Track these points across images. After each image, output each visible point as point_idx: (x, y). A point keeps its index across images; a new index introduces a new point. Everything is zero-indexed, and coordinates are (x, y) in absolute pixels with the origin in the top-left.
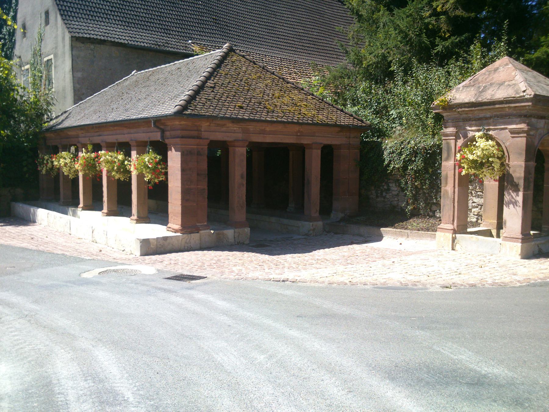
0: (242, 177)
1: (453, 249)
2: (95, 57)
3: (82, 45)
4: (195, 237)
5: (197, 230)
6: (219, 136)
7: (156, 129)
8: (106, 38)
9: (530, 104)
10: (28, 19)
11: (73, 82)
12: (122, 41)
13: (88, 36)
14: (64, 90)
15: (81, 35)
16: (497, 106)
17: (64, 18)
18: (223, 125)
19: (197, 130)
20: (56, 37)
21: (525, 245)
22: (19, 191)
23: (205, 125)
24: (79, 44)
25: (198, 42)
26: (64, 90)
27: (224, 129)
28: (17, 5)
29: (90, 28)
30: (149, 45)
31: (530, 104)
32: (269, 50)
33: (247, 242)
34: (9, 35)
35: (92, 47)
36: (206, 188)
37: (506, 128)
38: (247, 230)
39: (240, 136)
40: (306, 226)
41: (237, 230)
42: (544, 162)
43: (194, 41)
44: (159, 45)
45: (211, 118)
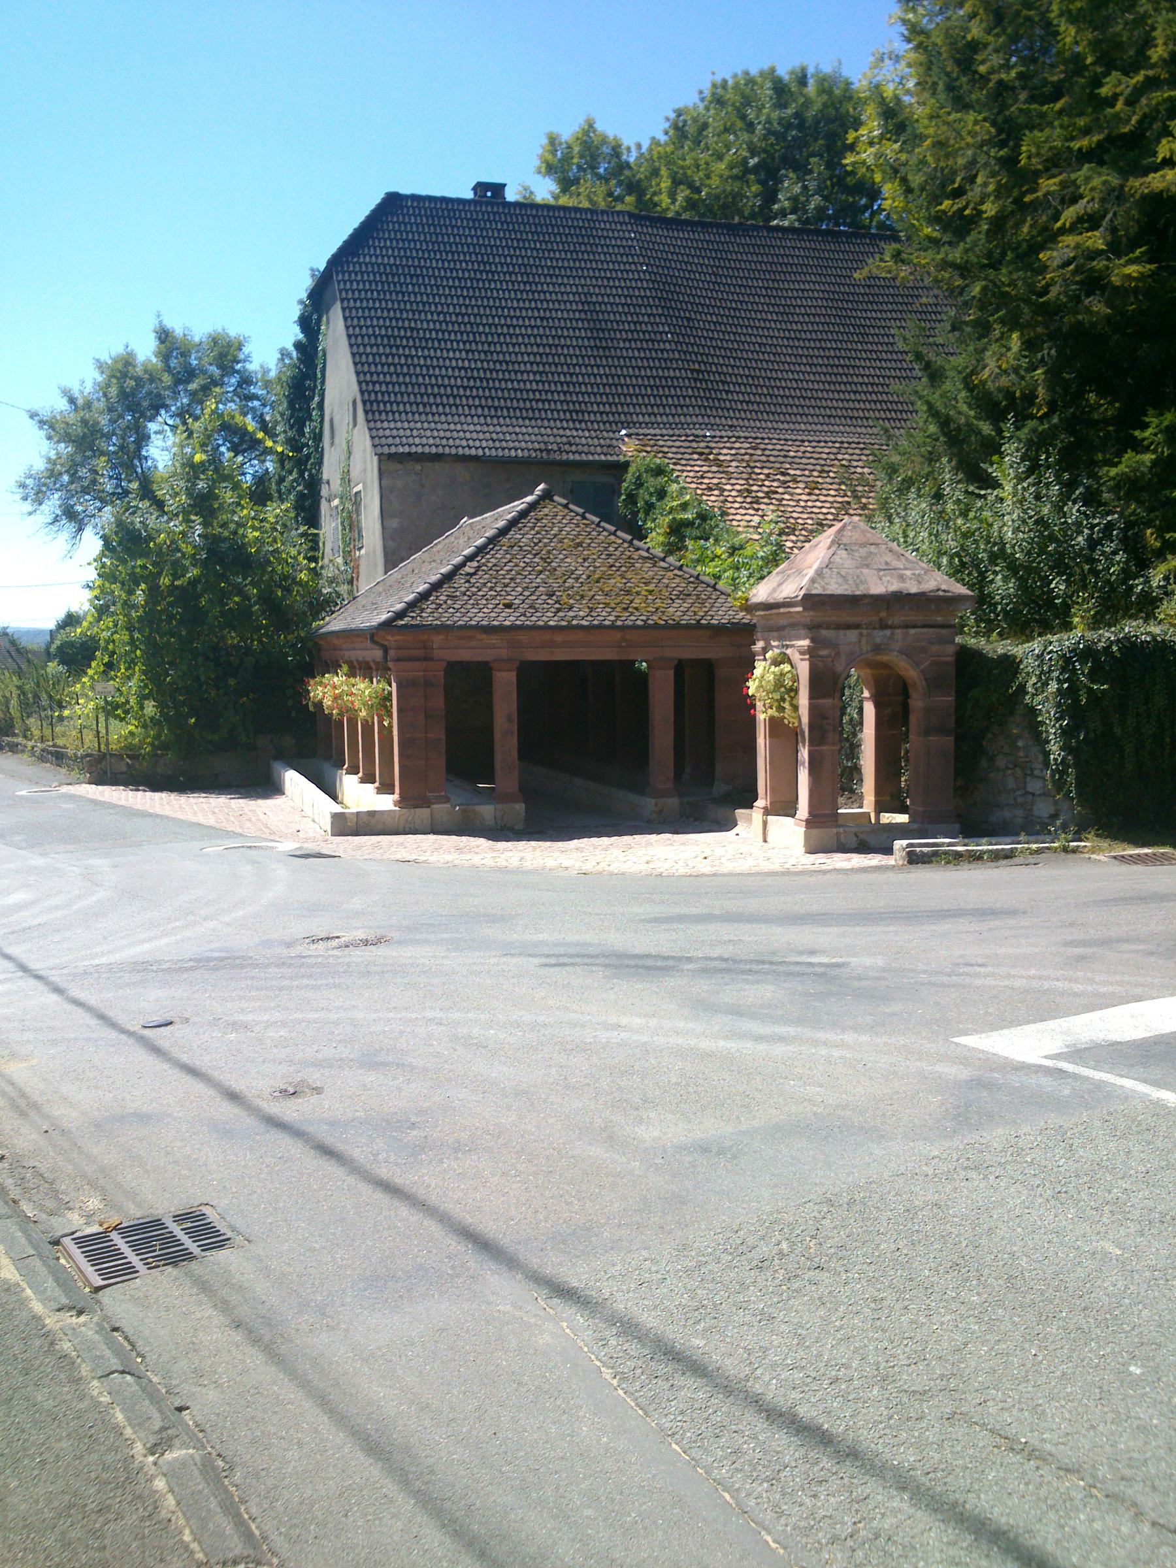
0: (509, 720)
1: (765, 841)
2: (423, 486)
3: (400, 466)
4: (423, 814)
5: (427, 803)
6: (465, 655)
7: (373, 646)
8: (440, 450)
9: (800, 609)
10: (335, 411)
11: (384, 538)
12: (473, 452)
13: (406, 449)
14: (374, 552)
15: (393, 450)
16: (782, 610)
17: (370, 417)
18: (470, 638)
19: (425, 648)
20: (364, 451)
21: (815, 831)
22: (288, 741)
23: (437, 640)
24: (392, 466)
25: (641, 431)
26: (374, 552)
27: (473, 643)
28: (323, 383)
29: (415, 433)
30: (526, 453)
31: (800, 609)
32: (819, 427)
33: (520, 826)
34: (315, 438)
35: (418, 467)
36: (443, 737)
37: (793, 646)
38: (520, 807)
39: (503, 653)
40: (649, 804)
41: (500, 806)
42: (908, 697)
43: (631, 431)
44: (548, 451)
45: (444, 629)
